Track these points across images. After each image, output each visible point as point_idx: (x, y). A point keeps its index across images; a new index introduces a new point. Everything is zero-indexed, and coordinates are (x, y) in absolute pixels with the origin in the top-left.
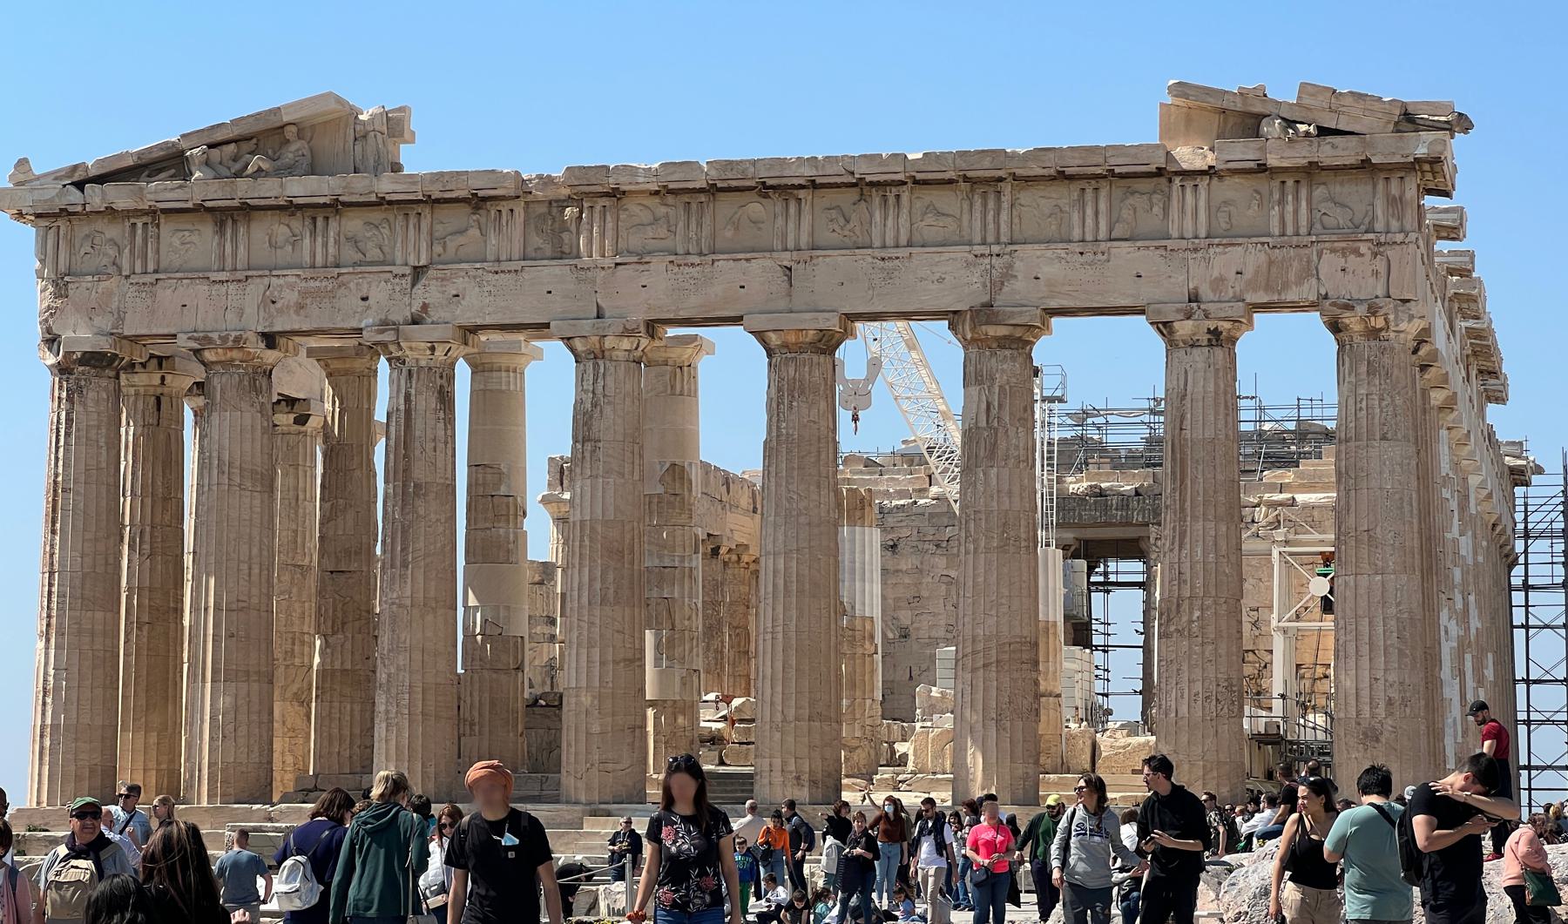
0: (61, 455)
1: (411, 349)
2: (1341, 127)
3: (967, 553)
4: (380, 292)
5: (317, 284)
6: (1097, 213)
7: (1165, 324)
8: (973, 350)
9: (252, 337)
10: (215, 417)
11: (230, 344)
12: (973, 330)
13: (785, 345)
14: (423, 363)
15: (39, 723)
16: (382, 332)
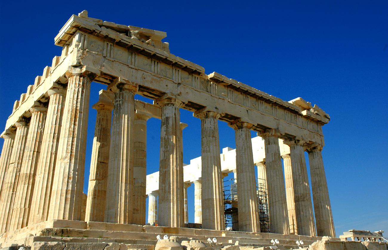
0: (79, 100)
1: (178, 102)
2: (319, 114)
3: (277, 178)
4: (171, 85)
5: (155, 78)
6: (289, 117)
7: (298, 141)
8: (273, 138)
9: (138, 85)
10: (126, 104)
11: (134, 85)
12: (275, 133)
13: (247, 127)
14: (178, 107)
15: (65, 189)
16: (172, 95)
